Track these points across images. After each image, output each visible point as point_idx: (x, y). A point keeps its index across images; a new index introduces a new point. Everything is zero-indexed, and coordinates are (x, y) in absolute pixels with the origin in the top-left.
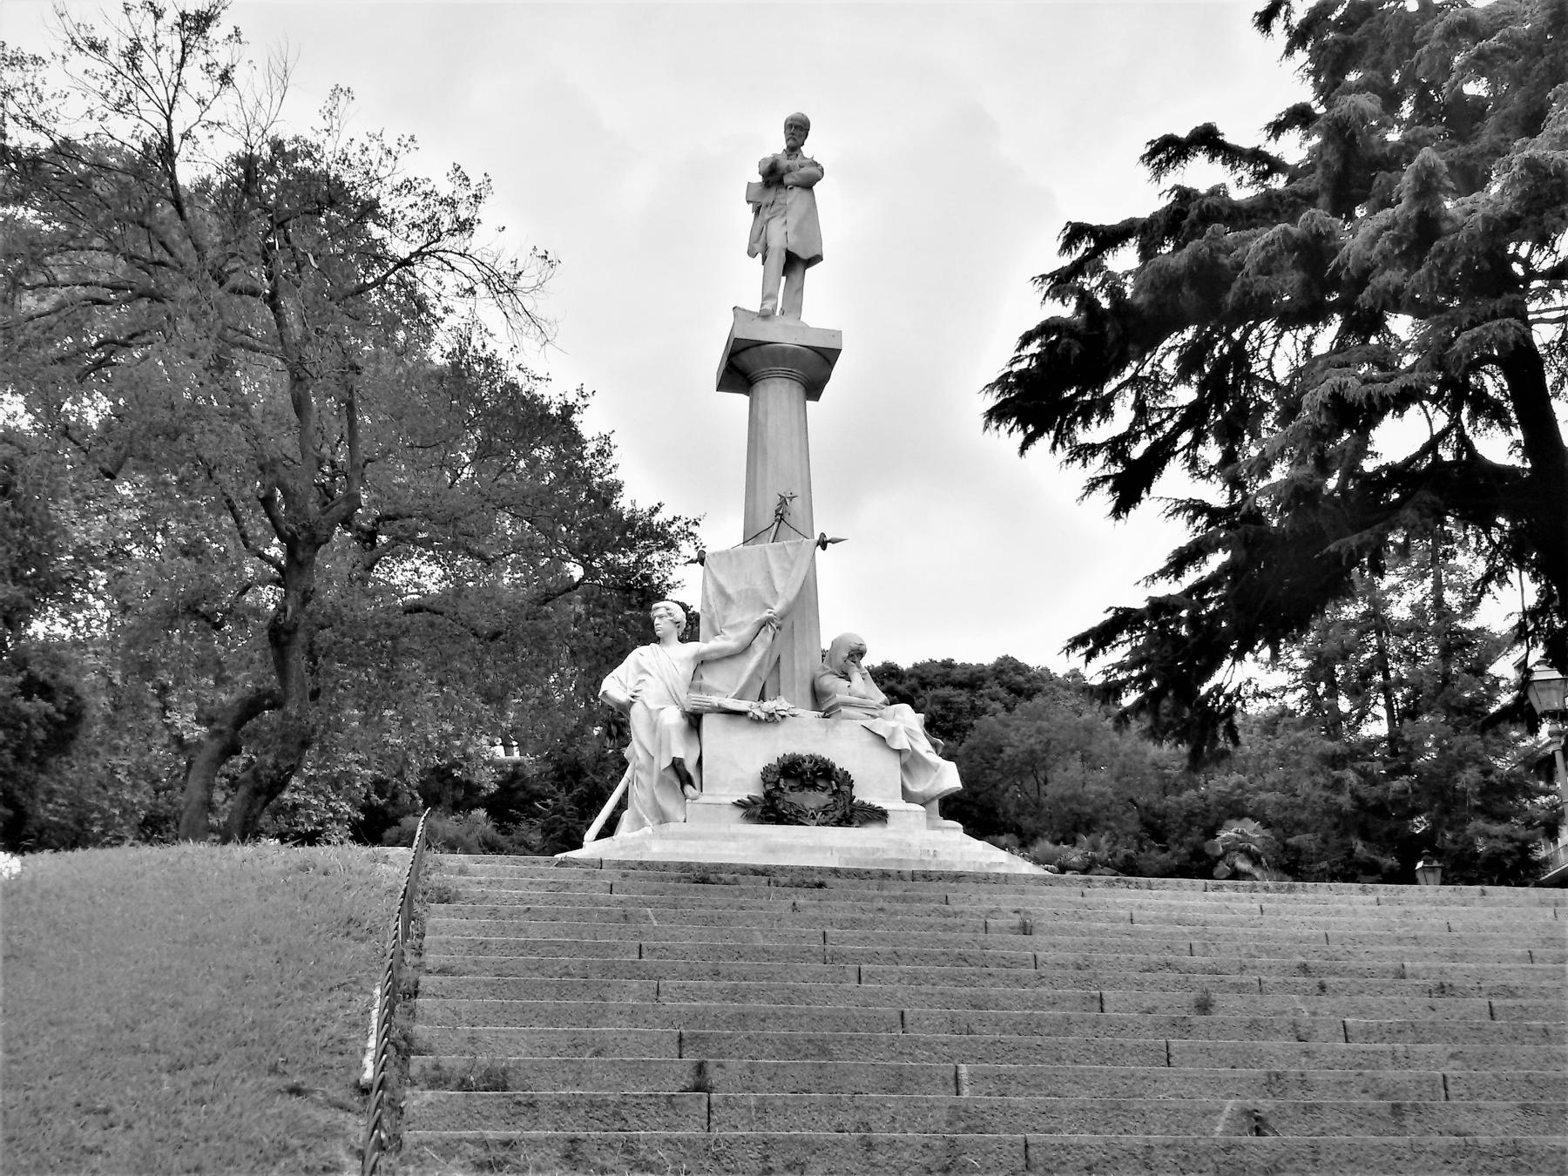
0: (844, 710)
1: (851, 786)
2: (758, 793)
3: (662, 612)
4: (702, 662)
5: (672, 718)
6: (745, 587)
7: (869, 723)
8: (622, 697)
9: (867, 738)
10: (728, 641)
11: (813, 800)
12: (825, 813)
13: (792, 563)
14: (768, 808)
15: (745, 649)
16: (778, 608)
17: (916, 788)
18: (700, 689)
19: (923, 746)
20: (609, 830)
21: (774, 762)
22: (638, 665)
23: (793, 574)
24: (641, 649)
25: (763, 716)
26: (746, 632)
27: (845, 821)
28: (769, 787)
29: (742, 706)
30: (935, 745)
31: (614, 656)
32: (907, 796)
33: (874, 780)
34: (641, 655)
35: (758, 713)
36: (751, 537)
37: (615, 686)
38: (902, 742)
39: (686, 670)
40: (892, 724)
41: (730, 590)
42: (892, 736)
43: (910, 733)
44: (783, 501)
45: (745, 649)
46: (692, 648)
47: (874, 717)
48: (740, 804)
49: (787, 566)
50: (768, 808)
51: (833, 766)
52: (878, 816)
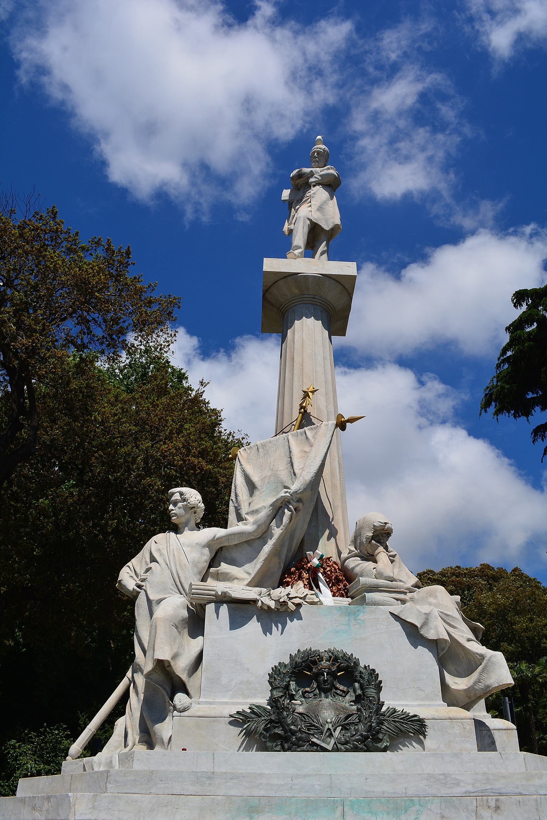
0: (369, 596)
1: (379, 688)
2: (262, 700)
3: (177, 497)
6: (269, 474)
7: (397, 609)
9: (398, 626)
10: (247, 527)
11: (328, 710)
12: (345, 728)
13: (311, 446)
16: (296, 486)
18: (218, 577)
19: (463, 634)
20: (95, 746)
21: (287, 661)
22: (151, 554)
23: (312, 455)
24: (159, 537)
25: (272, 604)
26: (263, 514)
28: (277, 694)
29: (252, 593)
30: (474, 630)
32: (448, 695)
34: (159, 543)
35: (267, 601)
36: (280, 431)
37: (127, 577)
38: (436, 630)
39: (206, 555)
40: (425, 609)
41: (255, 479)
42: (425, 624)
43: (445, 618)
44: (306, 395)
47: (403, 602)
49: (307, 449)
51: (357, 664)
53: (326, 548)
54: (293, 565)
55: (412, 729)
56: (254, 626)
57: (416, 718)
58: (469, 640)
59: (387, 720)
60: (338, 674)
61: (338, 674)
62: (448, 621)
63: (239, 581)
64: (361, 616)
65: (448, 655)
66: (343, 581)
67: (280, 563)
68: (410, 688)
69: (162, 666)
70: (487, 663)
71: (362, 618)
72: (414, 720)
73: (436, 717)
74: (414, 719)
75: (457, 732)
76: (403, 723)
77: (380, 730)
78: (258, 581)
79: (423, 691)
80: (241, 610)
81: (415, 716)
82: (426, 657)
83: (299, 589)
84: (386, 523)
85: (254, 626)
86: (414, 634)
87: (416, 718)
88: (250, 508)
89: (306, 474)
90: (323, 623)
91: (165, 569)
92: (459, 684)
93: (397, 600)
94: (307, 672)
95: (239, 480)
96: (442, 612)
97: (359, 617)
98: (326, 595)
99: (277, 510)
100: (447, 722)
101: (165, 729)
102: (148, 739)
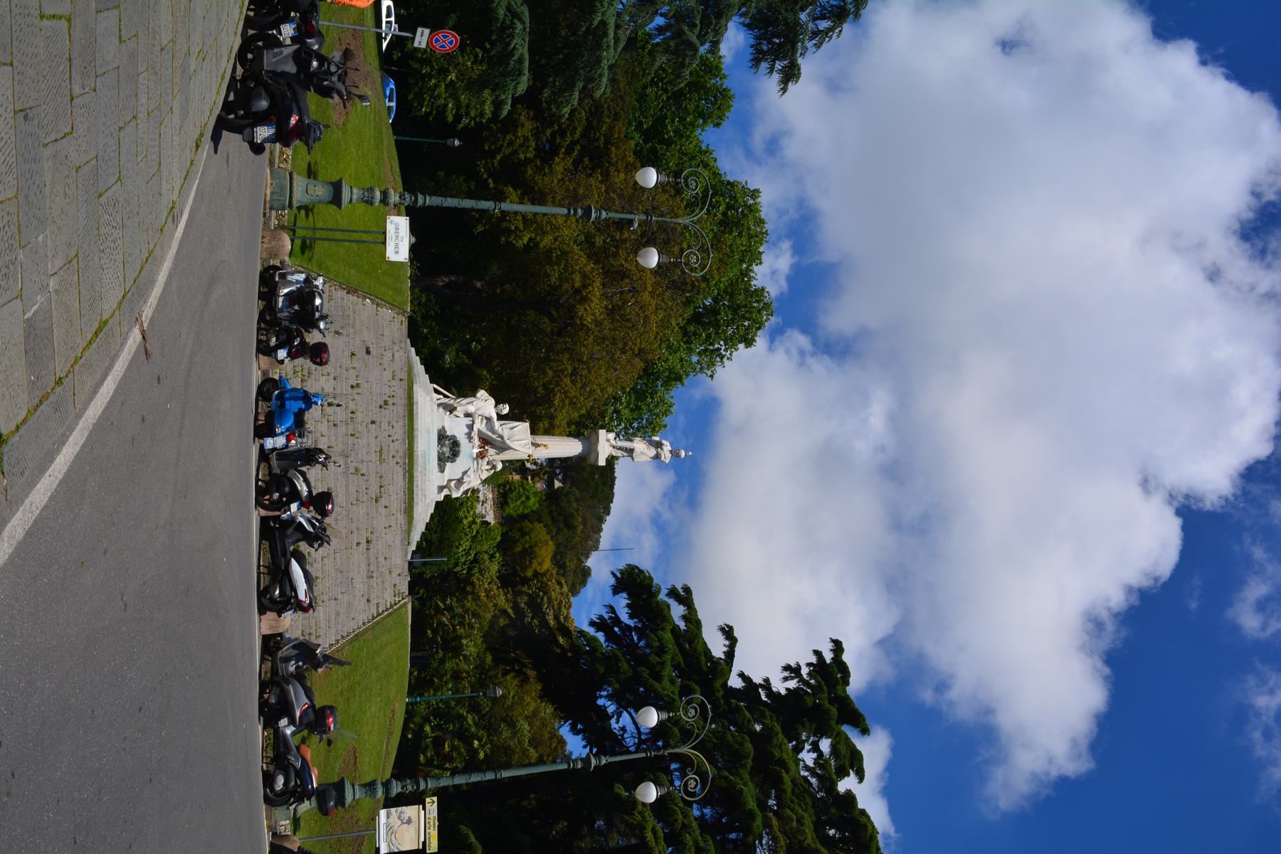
4: (489, 419)
5: (471, 409)
8: (478, 395)
14: (442, 436)
15: (494, 432)
17: (453, 484)
20: (436, 391)
27: (440, 459)
31: (492, 393)
32: (450, 481)
33: (453, 470)
34: (492, 401)
37: (482, 393)
38: (466, 479)
45: (494, 432)
46: (495, 417)
48: (443, 428)
50: (442, 436)
52: (442, 471)
53: (491, 451)
54: (485, 441)
55: (442, 470)
56: (467, 430)
63: (479, 425)
65: (460, 482)
66: (481, 455)
69: (455, 409)
77: (442, 461)
78: (479, 431)
80: (471, 427)
82: (459, 476)
83: (477, 441)
85: (467, 430)
86: (465, 473)
88: (504, 429)
89: (511, 445)
90: (469, 449)
91: (483, 404)
92: (453, 484)
94: (455, 444)
95: (516, 424)
98: (476, 450)
99: (501, 437)
101: (441, 410)
102: (439, 405)
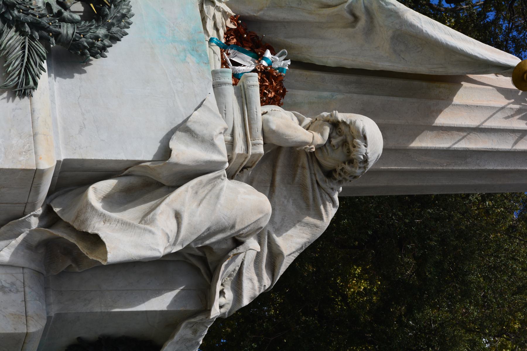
57: (32, 83)
58: (178, 216)
59: (25, 38)
60: (92, 5)
61: (92, 5)
62: (208, 197)
64: (192, 60)
67: (261, 10)
68: (83, 114)
70: (140, 228)
71: (188, 60)
72: (27, 83)
73: (36, 115)
74: (30, 77)
75: (14, 142)
76: (23, 61)
79: (80, 132)
81: (36, 84)
84: (365, 138)
87: (32, 83)
93: (233, 134)
96: (221, 189)
97: (189, 55)
100: (28, 129)
